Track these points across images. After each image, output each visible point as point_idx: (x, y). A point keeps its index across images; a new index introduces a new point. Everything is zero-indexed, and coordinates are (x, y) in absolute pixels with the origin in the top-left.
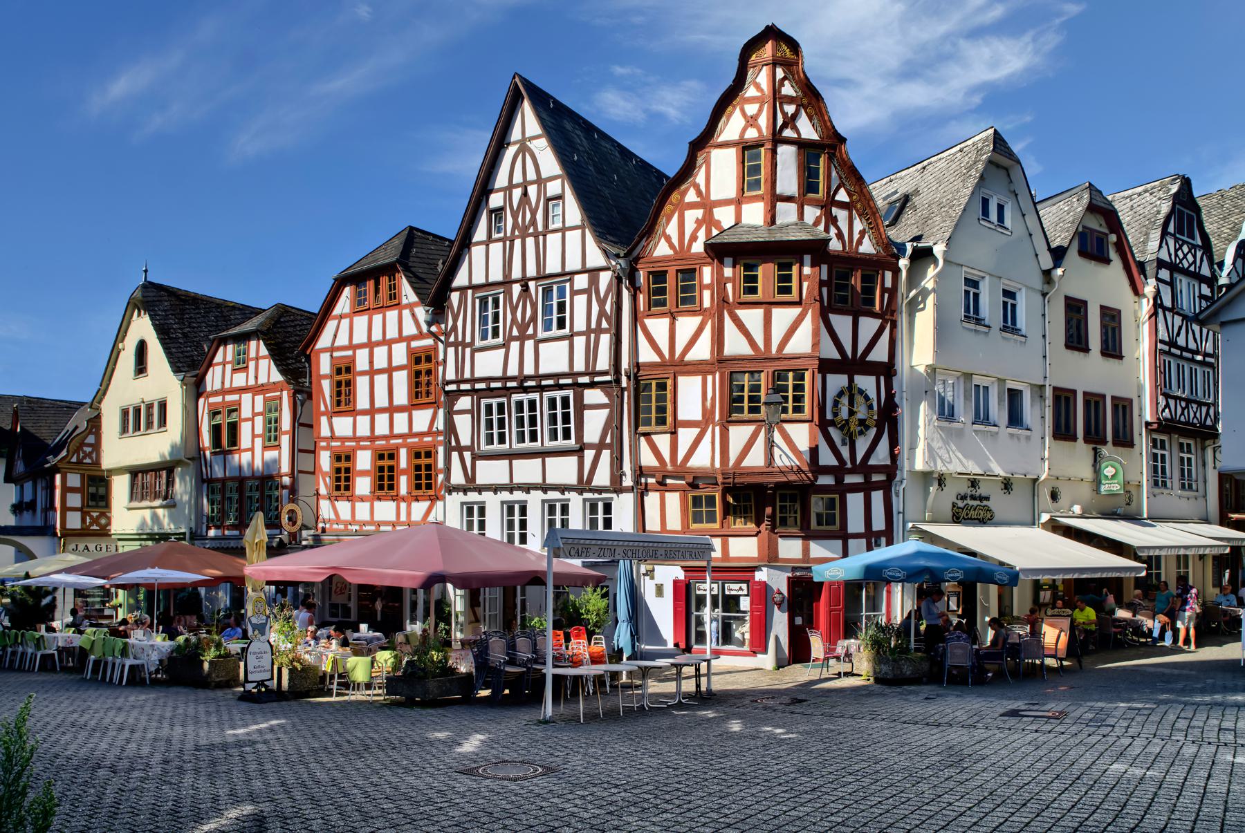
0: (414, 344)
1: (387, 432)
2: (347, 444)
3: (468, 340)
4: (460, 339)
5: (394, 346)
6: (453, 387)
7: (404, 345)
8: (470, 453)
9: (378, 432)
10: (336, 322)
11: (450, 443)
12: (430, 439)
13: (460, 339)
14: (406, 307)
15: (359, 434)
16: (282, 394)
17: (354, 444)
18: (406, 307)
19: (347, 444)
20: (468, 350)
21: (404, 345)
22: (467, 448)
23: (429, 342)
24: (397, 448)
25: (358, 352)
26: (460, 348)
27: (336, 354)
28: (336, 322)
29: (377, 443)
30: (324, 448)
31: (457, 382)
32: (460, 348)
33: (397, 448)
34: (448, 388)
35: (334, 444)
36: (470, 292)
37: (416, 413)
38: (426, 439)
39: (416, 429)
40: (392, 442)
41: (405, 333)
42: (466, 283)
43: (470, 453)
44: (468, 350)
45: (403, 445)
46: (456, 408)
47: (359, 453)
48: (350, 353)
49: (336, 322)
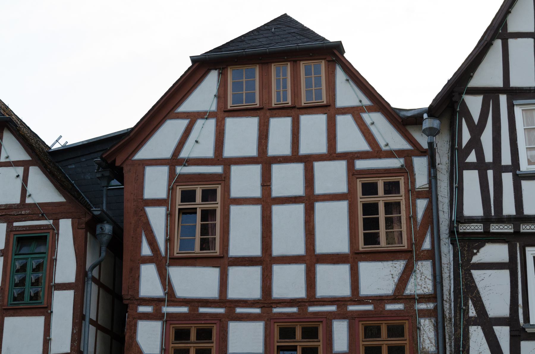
0: (361, 164)
1: (301, 293)
2: (202, 310)
3: (506, 159)
4: (489, 158)
5: (318, 166)
6: (478, 228)
7: (342, 165)
8: (508, 328)
9: (278, 293)
10: (182, 124)
11: (467, 311)
12: (399, 306)
13: (489, 158)
14: (344, 111)
15: (233, 294)
16: (57, 225)
17: (221, 311)
18: (344, 111)
19: (202, 310)
20: (507, 179)
21: (342, 165)
22: (500, 321)
23: (396, 163)
24: (329, 318)
25: (235, 169)
26: (490, 174)
27: (180, 170)
28: (184, 123)
29: (276, 310)
30: (146, 317)
31: (486, 220)
32: (490, 174)
33: (329, 318)
34: (465, 228)
35: (167, 310)
36: (503, 99)
37: (364, 267)
38: (389, 307)
39: (365, 290)
40: (312, 309)
41: (341, 148)
42: (499, 83)
43: (508, 328)
44: (507, 179)
45: (341, 315)
46: (475, 259)
47: (234, 327)
48: (218, 169)
49: (184, 123)
